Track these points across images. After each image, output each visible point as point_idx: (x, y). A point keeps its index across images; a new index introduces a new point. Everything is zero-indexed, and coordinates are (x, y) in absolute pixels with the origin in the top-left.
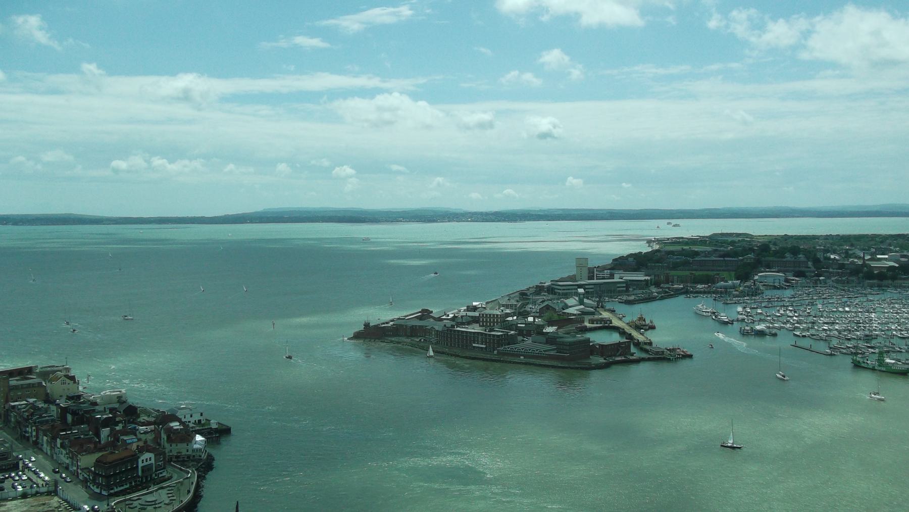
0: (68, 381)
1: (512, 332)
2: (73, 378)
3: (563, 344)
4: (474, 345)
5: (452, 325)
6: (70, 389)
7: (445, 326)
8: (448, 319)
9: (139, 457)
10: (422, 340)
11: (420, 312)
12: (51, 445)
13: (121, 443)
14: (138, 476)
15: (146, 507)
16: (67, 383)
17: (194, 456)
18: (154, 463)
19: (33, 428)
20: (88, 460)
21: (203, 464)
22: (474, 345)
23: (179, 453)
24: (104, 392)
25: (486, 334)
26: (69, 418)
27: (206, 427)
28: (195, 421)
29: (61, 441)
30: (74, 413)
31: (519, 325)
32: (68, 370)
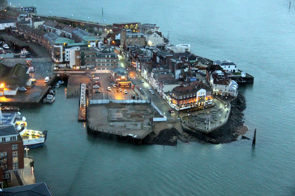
0: (157, 35)
2: (160, 34)
6: (160, 41)
9: (197, 91)
13: (187, 80)
16: (157, 37)
17: (229, 94)
18: (205, 95)
19: (139, 63)
20: (169, 88)
21: (235, 100)
23: (220, 90)
24: (178, 45)
26: (158, 59)
27: (238, 76)
28: (231, 70)
29: (154, 74)
30: (161, 58)
32: (158, 28)
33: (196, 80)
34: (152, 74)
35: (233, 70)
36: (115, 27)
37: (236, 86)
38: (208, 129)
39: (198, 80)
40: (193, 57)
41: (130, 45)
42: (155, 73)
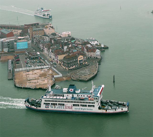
0: (51, 28)
2: (52, 27)
9: (78, 57)
12: (48, 51)
14: (78, 63)
15: (81, 75)
17: (96, 57)
20: (61, 57)
23: (91, 56)
24: (63, 33)
26: (53, 41)
30: (54, 40)
32: (50, 24)
33: (76, 51)
34: (51, 50)
36: (25, 26)
37: (99, 52)
38: (87, 78)
39: (77, 51)
40: (73, 39)
41: (35, 35)
42: (52, 49)
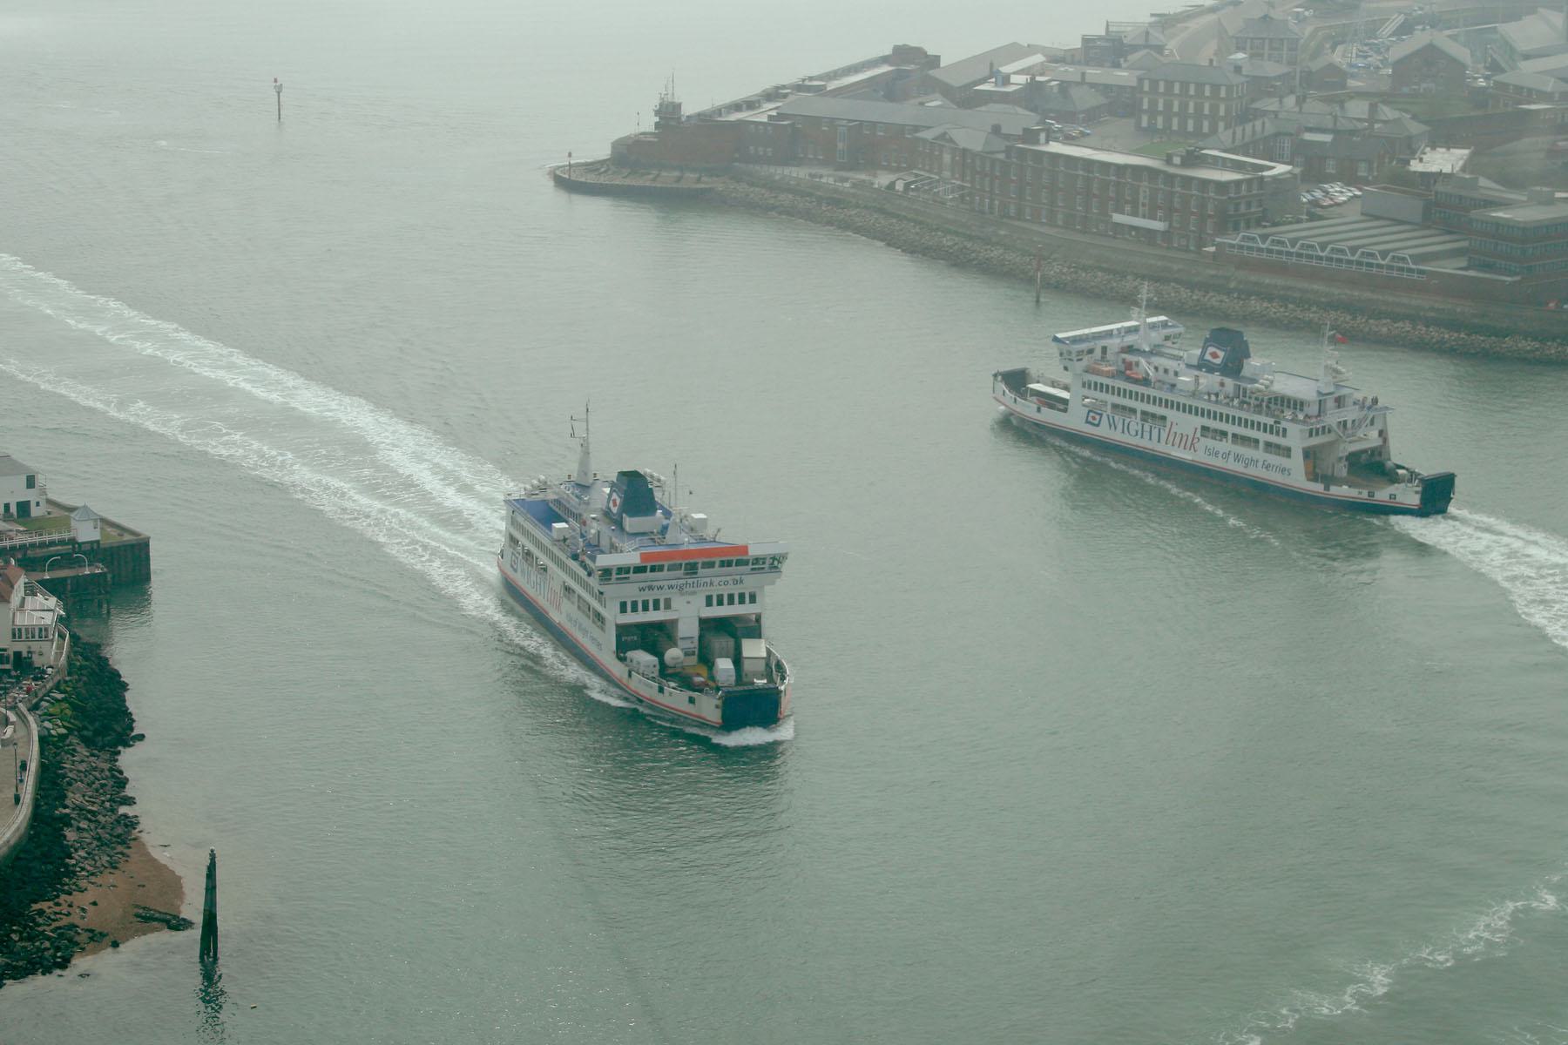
1: (1281, 169)
3: (1501, 231)
4: (1118, 218)
5: (1026, 130)
7: (996, 130)
8: (1004, 98)
10: (900, 186)
11: (885, 60)
22: (1118, 218)
25: (1173, 176)
27: (56, 537)
28: (7, 506)
31: (1308, 136)
35: (18, 504)
